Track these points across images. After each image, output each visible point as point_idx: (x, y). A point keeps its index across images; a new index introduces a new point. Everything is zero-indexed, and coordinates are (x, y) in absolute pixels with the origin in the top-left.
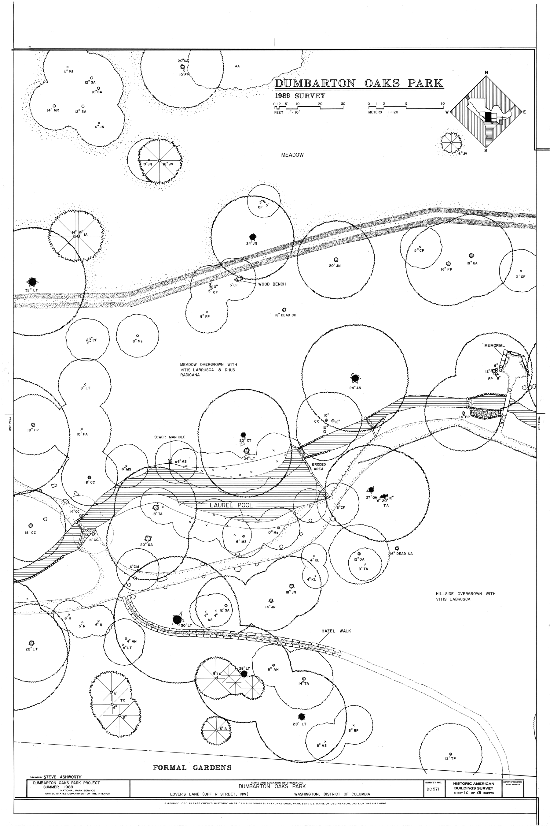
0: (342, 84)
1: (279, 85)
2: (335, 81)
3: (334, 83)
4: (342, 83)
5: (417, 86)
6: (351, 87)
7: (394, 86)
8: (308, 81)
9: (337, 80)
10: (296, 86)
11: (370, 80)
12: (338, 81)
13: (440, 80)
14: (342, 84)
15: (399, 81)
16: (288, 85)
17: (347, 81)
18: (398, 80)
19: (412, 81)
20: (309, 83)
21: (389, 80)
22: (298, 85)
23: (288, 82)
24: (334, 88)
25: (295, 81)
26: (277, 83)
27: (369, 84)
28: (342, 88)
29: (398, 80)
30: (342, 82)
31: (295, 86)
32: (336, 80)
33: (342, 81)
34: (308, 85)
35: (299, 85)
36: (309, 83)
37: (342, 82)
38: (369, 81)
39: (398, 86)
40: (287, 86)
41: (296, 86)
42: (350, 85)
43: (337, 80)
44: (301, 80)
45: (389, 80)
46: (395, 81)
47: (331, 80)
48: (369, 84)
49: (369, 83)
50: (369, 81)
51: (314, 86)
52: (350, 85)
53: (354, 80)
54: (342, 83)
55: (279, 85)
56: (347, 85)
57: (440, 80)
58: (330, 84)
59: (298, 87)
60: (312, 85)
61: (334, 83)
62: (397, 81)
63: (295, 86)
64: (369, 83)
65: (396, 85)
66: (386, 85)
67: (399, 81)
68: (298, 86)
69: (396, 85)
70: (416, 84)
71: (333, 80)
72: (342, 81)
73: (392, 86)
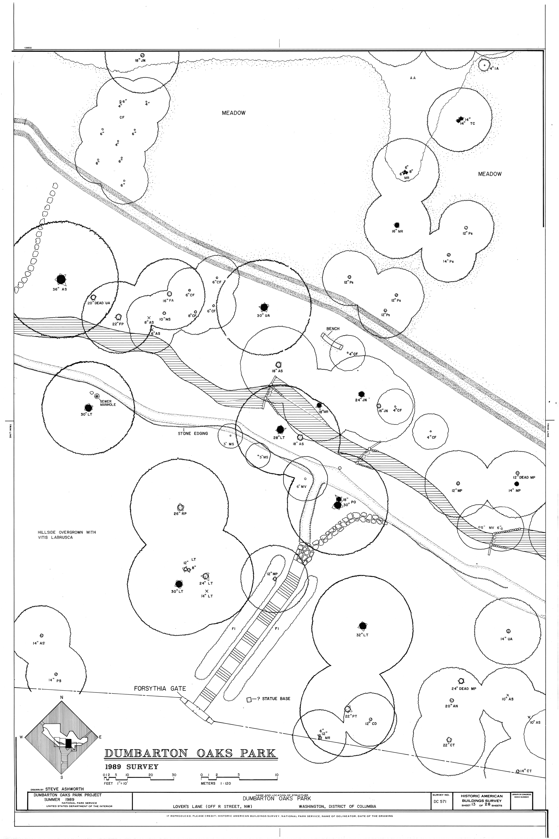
0: (174, 754)
1: (109, 755)
2: (167, 751)
3: (165, 753)
4: (174, 753)
5: (250, 756)
6: (183, 756)
7: (226, 756)
8: (138, 751)
9: (168, 750)
10: (126, 755)
11: (203, 750)
12: (170, 751)
14: (174, 754)
15: (231, 751)
16: (119, 755)
17: (179, 751)
18: (231, 750)
19: (245, 751)
20: (139, 753)
21: (222, 750)
22: (129, 755)
23: (119, 752)
25: (125, 751)
26: (107, 753)
27: (201, 754)
30: (174, 752)
31: (125, 756)
32: (167, 750)
33: (174, 751)
34: (138, 755)
35: (130, 755)
36: (139, 753)
37: (174, 752)
38: (201, 751)
39: (231, 756)
40: (117, 756)
41: (126, 755)
42: (182, 755)
43: (168, 750)
44: (131, 750)
45: (222, 750)
46: (228, 751)
47: (163, 750)
48: (201, 754)
49: (201, 753)
50: (201, 751)
51: (145, 756)
52: (182, 755)
53: (186, 750)
54: (174, 753)
55: (109, 754)
58: (162, 754)
59: (129, 757)
61: (165, 753)
62: (230, 751)
63: (125, 756)
64: (201, 753)
65: (229, 755)
66: (271, 755)
67: (231, 751)
68: (128, 756)
69: (229, 755)
70: (248, 754)
71: (165, 750)
72: (174, 751)
73: (225, 756)
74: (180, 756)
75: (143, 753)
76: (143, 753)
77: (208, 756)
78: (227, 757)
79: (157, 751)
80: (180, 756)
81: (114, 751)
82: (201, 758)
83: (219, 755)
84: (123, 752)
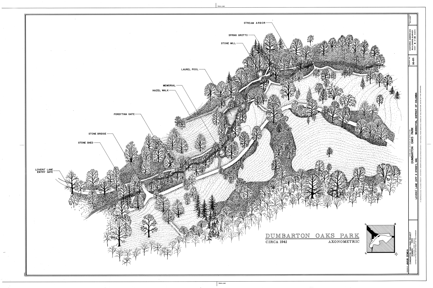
1: (268, 237)
3: (298, 236)
5: (345, 237)
7: (331, 237)
8: (284, 235)
12: (300, 234)
13: (358, 234)
17: (305, 235)
18: (334, 234)
19: (342, 235)
20: (284, 236)
21: (329, 234)
23: (273, 235)
24: (298, 238)
26: (267, 236)
28: (303, 238)
29: (334, 234)
31: (277, 237)
33: (303, 235)
34: (284, 237)
35: (279, 237)
36: (284, 236)
38: (318, 235)
41: (277, 237)
42: (307, 237)
45: (329, 234)
46: (332, 234)
50: (318, 235)
51: (287, 237)
52: (307, 237)
53: (309, 234)
56: (305, 237)
57: (358, 234)
58: (296, 236)
59: (278, 238)
60: (286, 237)
61: (298, 236)
62: (333, 235)
63: (277, 237)
66: (328, 237)
70: (344, 236)
72: (303, 235)
73: (331, 237)
74: (306, 237)
75: (286, 236)
76: (286, 236)
77: (321, 237)
78: (332, 238)
79: (293, 235)
80: (306, 237)
81: (270, 235)
82: (317, 238)
83: (328, 237)
84: (275, 235)
